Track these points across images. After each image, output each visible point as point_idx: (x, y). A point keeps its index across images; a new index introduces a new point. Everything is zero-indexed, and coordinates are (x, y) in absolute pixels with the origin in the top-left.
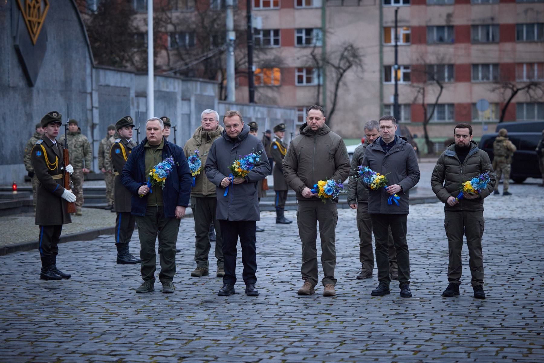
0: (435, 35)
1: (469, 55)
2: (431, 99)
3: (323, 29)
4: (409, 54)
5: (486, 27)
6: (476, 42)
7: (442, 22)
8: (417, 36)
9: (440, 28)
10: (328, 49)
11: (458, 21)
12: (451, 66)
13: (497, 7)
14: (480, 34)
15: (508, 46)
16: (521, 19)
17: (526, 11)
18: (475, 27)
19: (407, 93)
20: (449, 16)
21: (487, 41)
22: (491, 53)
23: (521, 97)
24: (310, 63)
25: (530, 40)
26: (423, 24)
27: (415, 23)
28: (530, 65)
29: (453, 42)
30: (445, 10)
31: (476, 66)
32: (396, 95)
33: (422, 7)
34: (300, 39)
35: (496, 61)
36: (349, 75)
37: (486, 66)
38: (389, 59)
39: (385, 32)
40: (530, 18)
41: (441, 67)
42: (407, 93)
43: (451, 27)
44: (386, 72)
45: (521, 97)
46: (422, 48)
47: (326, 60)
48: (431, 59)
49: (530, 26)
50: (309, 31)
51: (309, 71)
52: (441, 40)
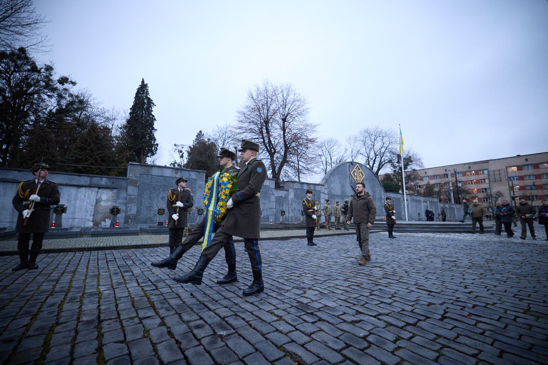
0: (529, 188)
3: (490, 188)
7: (531, 184)
10: (492, 192)
11: (536, 184)
12: (536, 196)
24: (486, 196)
27: (521, 185)
32: (515, 203)
33: (523, 181)
34: (483, 191)
38: (512, 195)
39: (512, 188)
41: (533, 196)
43: (534, 185)
47: (491, 196)
50: (485, 189)
51: (487, 199)
52: (532, 189)
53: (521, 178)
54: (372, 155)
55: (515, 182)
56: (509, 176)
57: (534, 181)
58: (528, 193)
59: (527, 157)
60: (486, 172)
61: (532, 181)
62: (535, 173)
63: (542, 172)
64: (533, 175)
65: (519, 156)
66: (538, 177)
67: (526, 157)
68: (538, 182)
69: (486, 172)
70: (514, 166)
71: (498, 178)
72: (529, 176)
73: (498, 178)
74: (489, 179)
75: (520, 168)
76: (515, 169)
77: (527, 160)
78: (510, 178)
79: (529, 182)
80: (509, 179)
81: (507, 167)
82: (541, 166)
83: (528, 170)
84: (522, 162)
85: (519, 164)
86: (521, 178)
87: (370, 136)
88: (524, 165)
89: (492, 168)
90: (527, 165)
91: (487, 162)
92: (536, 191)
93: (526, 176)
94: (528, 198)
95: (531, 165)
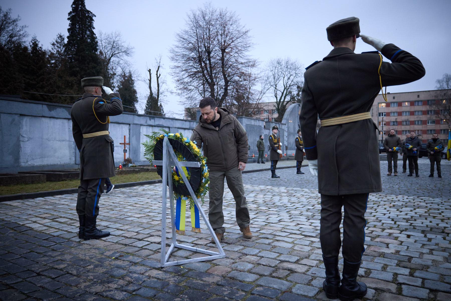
0: (392, 123)
1: (401, 128)
5: (406, 121)
6: (404, 125)
7: (394, 120)
8: (387, 124)
9: (394, 122)
11: (398, 120)
13: (409, 117)
14: (404, 123)
15: (412, 126)
16: (416, 119)
17: (417, 117)
18: (403, 121)
20: (396, 119)
21: (406, 125)
22: (408, 128)
25: (418, 124)
26: (389, 121)
27: (387, 121)
28: (418, 131)
29: (397, 125)
31: (403, 131)
32: (382, 138)
35: (409, 129)
40: (418, 119)
43: (396, 122)
46: (389, 126)
49: (418, 121)
52: (394, 125)
53: (388, 114)
55: (385, 118)
56: (380, 112)
57: (396, 117)
59: (395, 95)
62: (399, 111)
63: (403, 110)
64: (396, 112)
66: (400, 114)
68: (400, 119)
70: (384, 103)
72: (394, 112)
75: (388, 105)
76: (384, 105)
77: (394, 98)
78: (380, 113)
79: (392, 118)
81: (379, 103)
82: (403, 104)
83: (394, 107)
86: (388, 114)
90: (394, 103)
92: (397, 127)
93: (391, 112)
95: (396, 102)
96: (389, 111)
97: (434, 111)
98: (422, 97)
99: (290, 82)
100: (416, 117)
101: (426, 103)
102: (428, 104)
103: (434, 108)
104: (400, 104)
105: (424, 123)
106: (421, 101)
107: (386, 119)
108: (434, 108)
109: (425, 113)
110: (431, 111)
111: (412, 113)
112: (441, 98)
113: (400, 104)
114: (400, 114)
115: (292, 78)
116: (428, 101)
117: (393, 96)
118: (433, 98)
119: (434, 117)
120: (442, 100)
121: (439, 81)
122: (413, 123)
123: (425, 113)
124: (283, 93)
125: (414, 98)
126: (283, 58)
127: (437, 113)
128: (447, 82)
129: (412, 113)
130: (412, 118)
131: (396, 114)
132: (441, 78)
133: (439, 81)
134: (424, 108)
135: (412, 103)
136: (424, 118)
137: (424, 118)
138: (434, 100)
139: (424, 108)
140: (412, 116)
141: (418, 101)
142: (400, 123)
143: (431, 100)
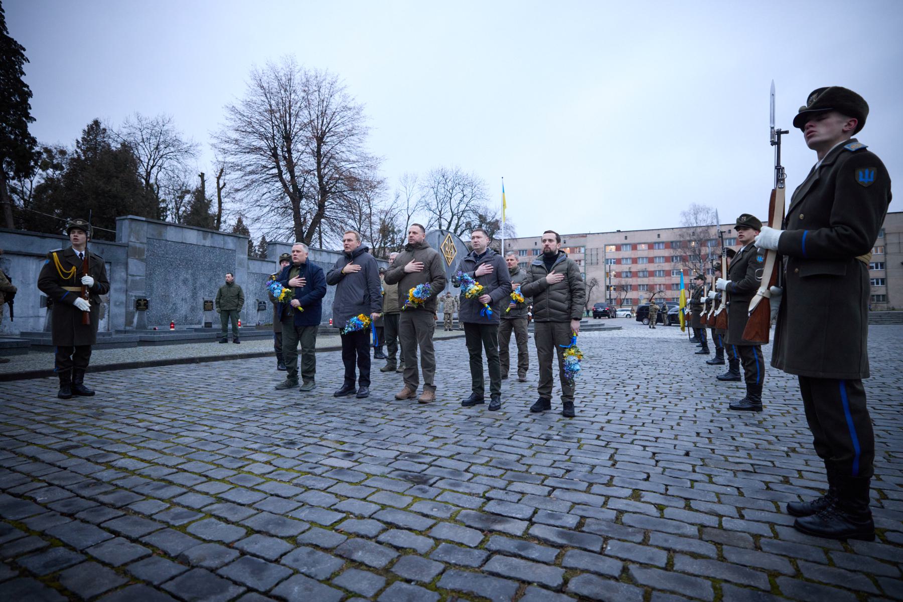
2: (623, 297)
4: (615, 281)
11: (632, 270)
14: (641, 274)
19: (614, 294)
22: (646, 281)
23: (656, 296)
25: (660, 276)
30: (628, 266)
36: (594, 289)
37: (643, 285)
38: (608, 284)
39: (607, 274)
41: (627, 286)
42: (614, 294)
44: (608, 288)
45: (656, 296)
48: (623, 283)
53: (618, 261)
54: (448, 216)
55: (613, 266)
58: (623, 281)
60: (582, 250)
61: (628, 266)
62: (633, 256)
65: (619, 231)
66: (635, 261)
67: (626, 234)
68: (635, 268)
69: (582, 250)
71: (594, 261)
73: (594, 261)
74: (585, 260)
75: (618, 248)
76: (613, 248)
77: (626, 238)
79: (624, 267)
80: (607, 261)
82: (639, 247)
84: (620, 239)
85: (619, 242)
86: (618, 261)
87: (449, 184)
88: (623, 245)
89: (591, 244)
90: (626, 245)
91: (584, 236)
94: (621, 288)
96: (620, 257)
97: (681, 256)
98: (665, 237)
99: (462, 207)
100: (656, 265)
101: (669, 245)
102: (672, 248)
103: (679, 252)
104: (634, 247)
105: (668, 273)
106: (663, 243)
107: (615, 268)
108: (679, 252)
109: (668, 259)
110: (676, 257)
111: (651, 260)
112: (688, 238)
113: (634, 247)
114: (635, 261)
115: (466, 200)
116: (672, 242)
117: (625, 234)
118: (678, 238)
119: (681, 267)
120: (690, 241)
121: (684, 214)
122: (652, 274)
123: (668, 259)
124: (450, 223)
125: (654, 239)
126: (449, 167)
127: (684, 259)
128: (695, 214)
129: (651, 260)
130: (651, 267)
131: (629, 261)
132: (686, 209)
133: (684, 214)
134: (667, 253)
135: (651, 246)
136: (667, 266)
137: (667, 266)
138: (680, 242)
139: (667, 253)
140: (652, 265)
141: (659, 243)
142: (635, 274)
143: (676, 242)
